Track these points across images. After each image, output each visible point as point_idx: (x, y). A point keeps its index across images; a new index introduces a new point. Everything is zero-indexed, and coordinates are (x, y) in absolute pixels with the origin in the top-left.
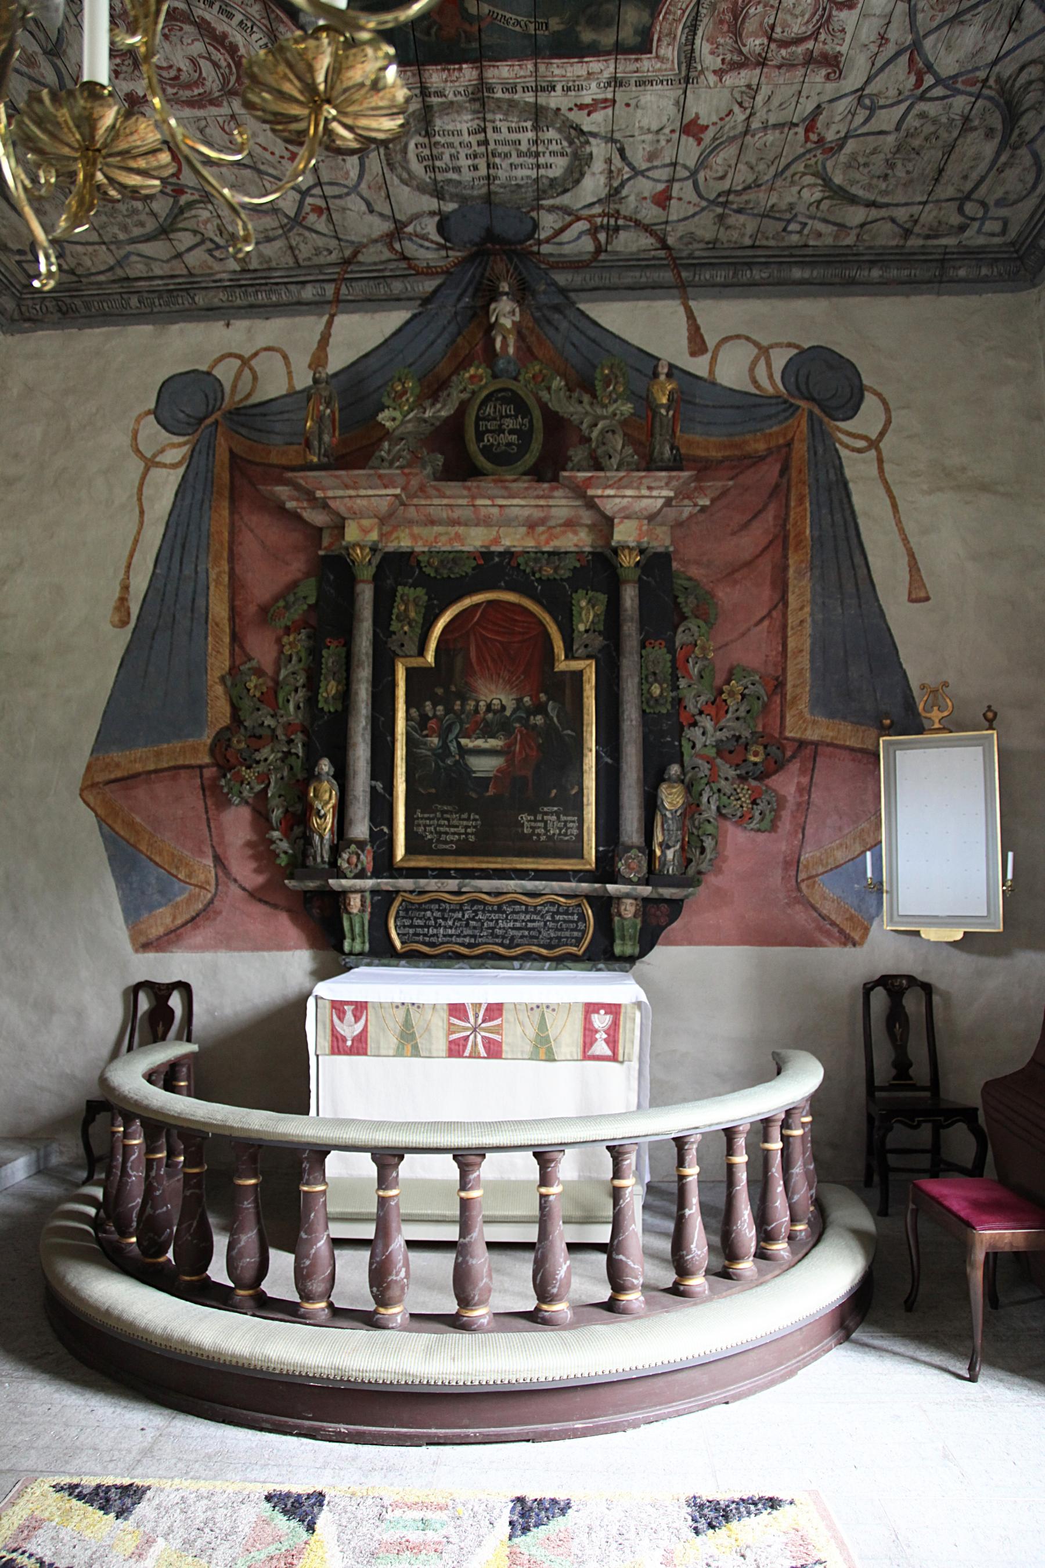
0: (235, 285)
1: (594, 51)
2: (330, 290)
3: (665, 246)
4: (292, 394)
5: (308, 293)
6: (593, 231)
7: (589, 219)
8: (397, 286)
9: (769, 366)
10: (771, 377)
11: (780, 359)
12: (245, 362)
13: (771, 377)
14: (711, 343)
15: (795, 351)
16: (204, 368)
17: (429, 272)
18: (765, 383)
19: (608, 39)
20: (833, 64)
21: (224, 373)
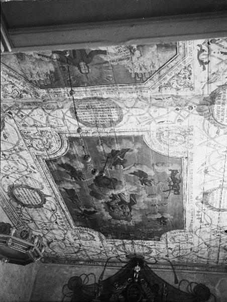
0: (87, 261)
1: (151, 240)
2: (105, 263)
3: (169, 261)
4: (95, 283)
5: (100, 264)
6: (155, 259)
7: (154, 258)
8: (118, 264)
9: (191, 287)
10: (191, 289)
11: (193, 285)
12: (87, 276)
13: (191, 289)
14: (179, 282)
15: (196, 285)
16: (79, 276)
17: (124, 262)
18: (190, 291)
19: (153, 239)
20: (192, 244)
21: (83, 277)
